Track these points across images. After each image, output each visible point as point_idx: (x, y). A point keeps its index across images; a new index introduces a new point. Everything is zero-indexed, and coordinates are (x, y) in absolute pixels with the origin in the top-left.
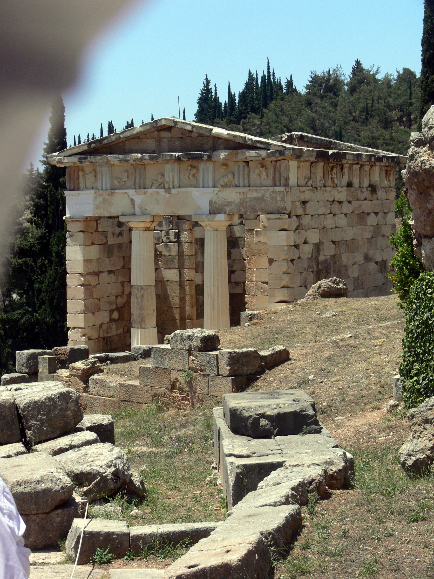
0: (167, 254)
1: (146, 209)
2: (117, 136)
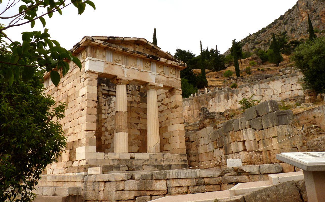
1: (129, 76)
2: (122, 39)
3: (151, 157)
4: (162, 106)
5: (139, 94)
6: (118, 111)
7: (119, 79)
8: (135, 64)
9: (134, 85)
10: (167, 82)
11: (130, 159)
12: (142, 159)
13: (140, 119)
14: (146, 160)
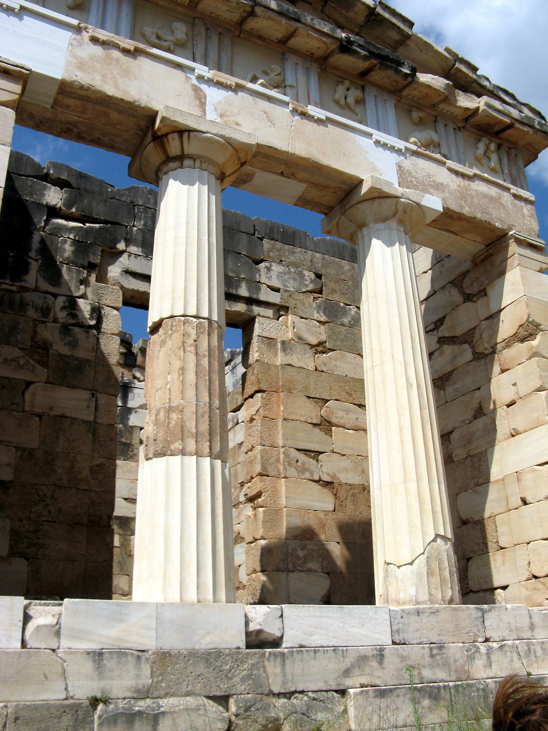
0: (65, 351)
1: (237, 124)
3: (398, 631)
4: (442, 353)
5: (319, 307)
6: (162, 320)
7: (166, 135)
8: (273, 75)
9: (296, 266)
10: (463, 195)
11: (249, 646)
12: (335, 649)
13: (329, 432)
14: (363, 659)
